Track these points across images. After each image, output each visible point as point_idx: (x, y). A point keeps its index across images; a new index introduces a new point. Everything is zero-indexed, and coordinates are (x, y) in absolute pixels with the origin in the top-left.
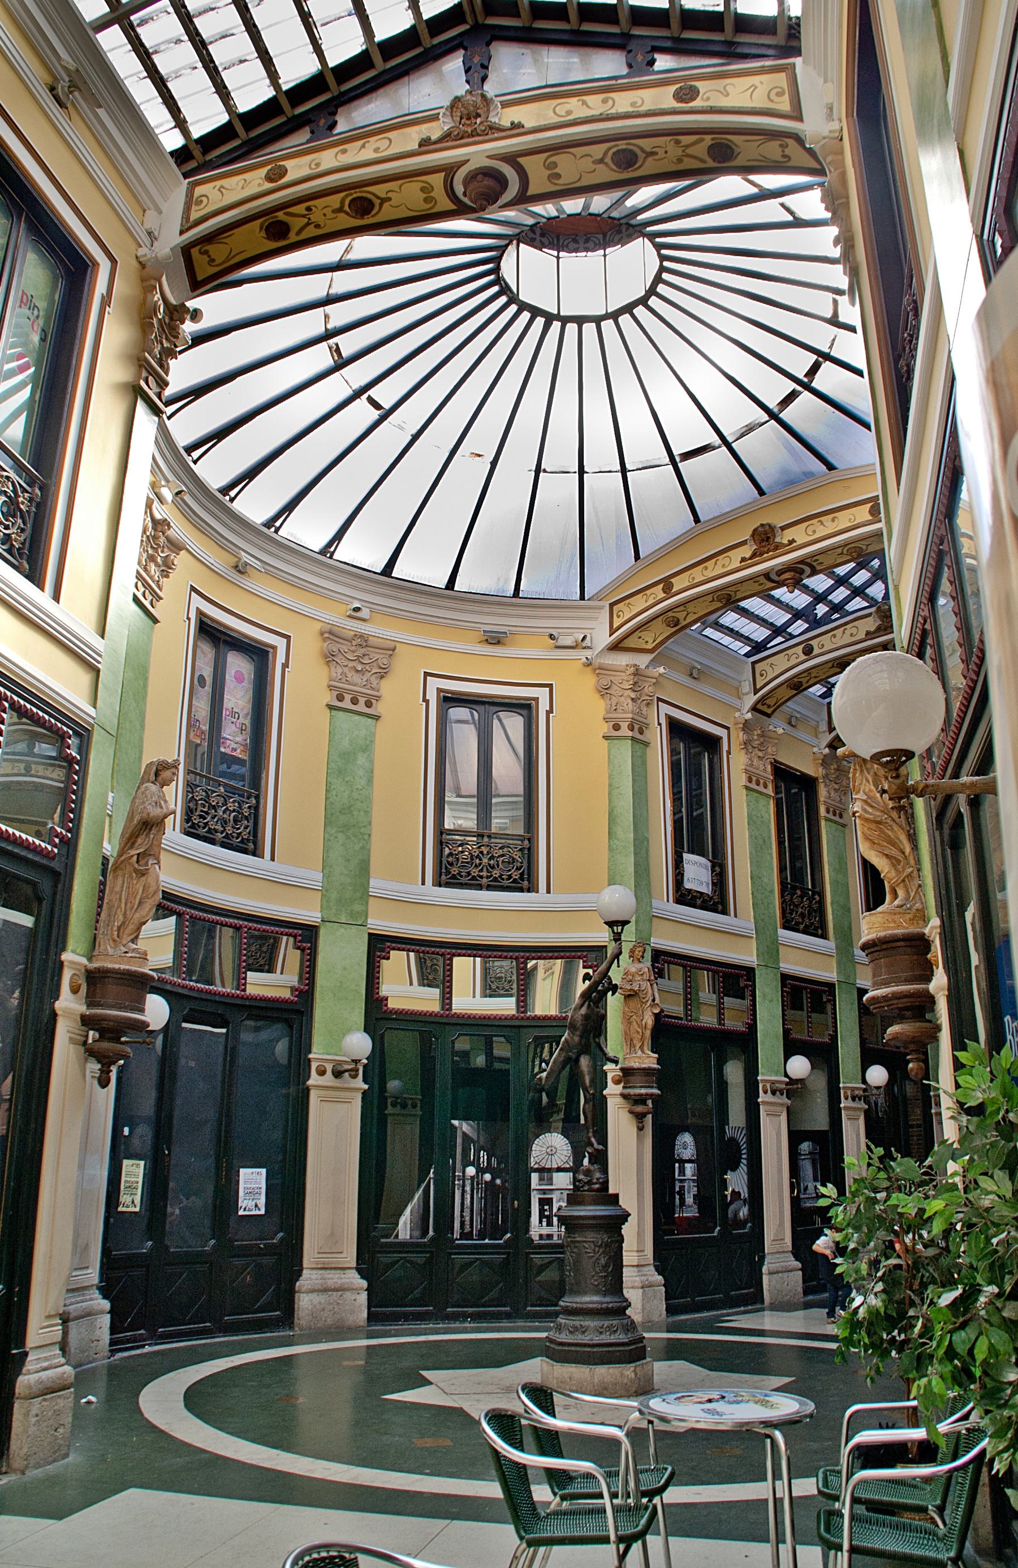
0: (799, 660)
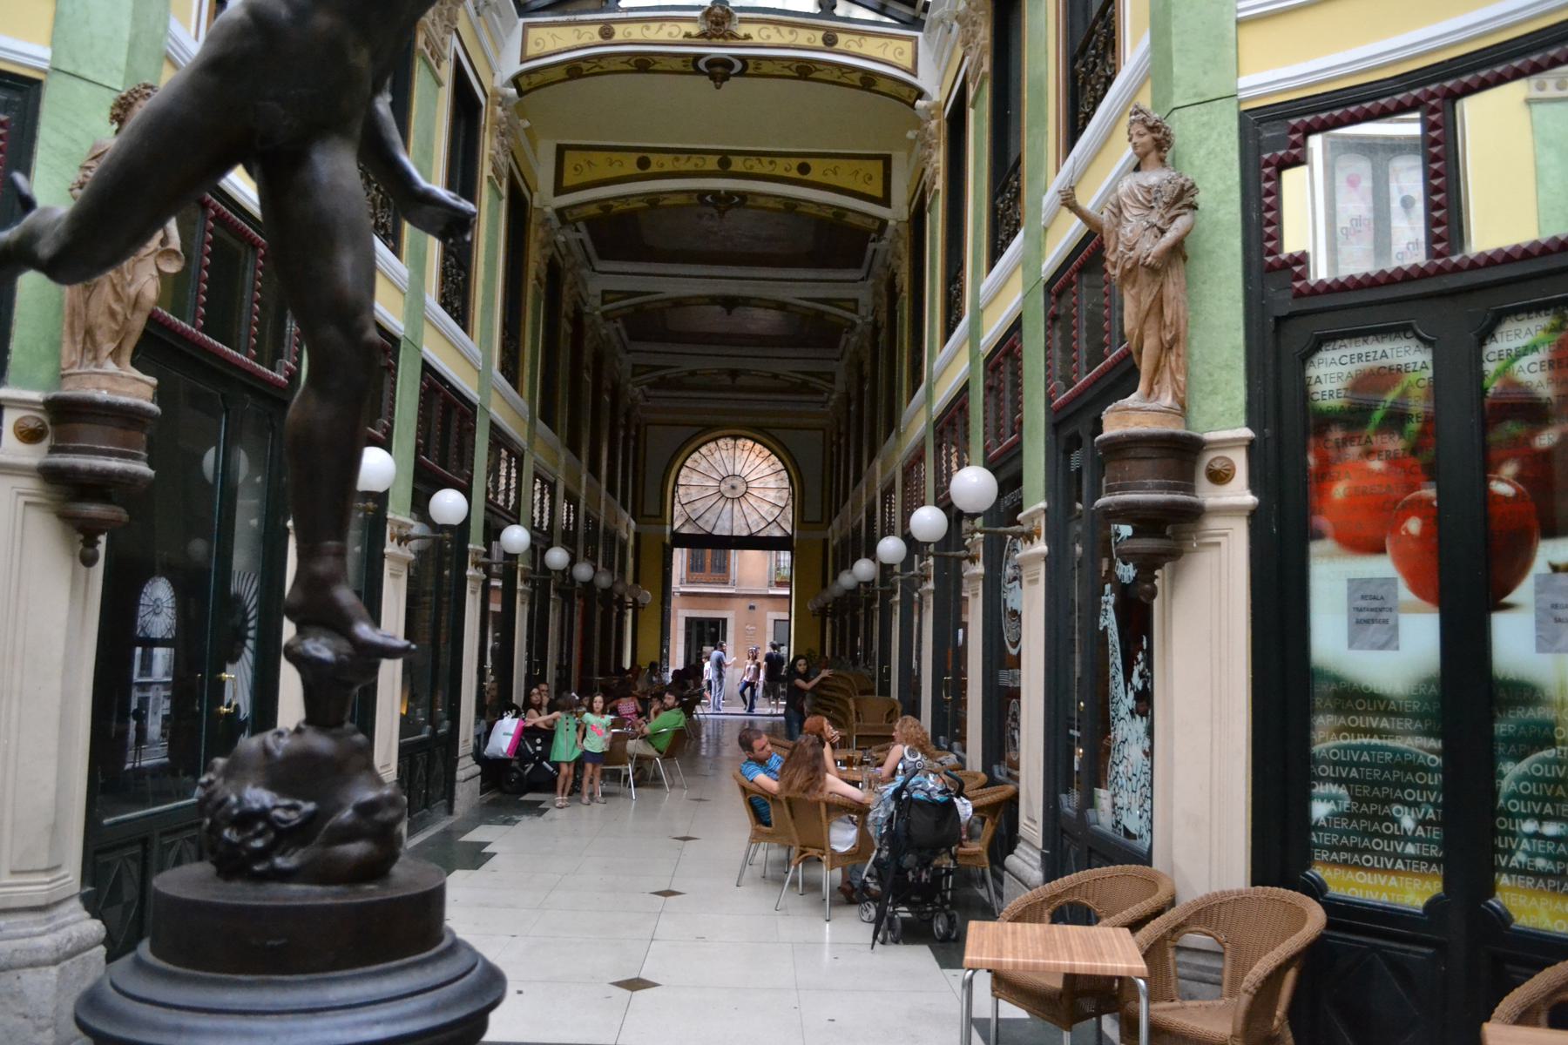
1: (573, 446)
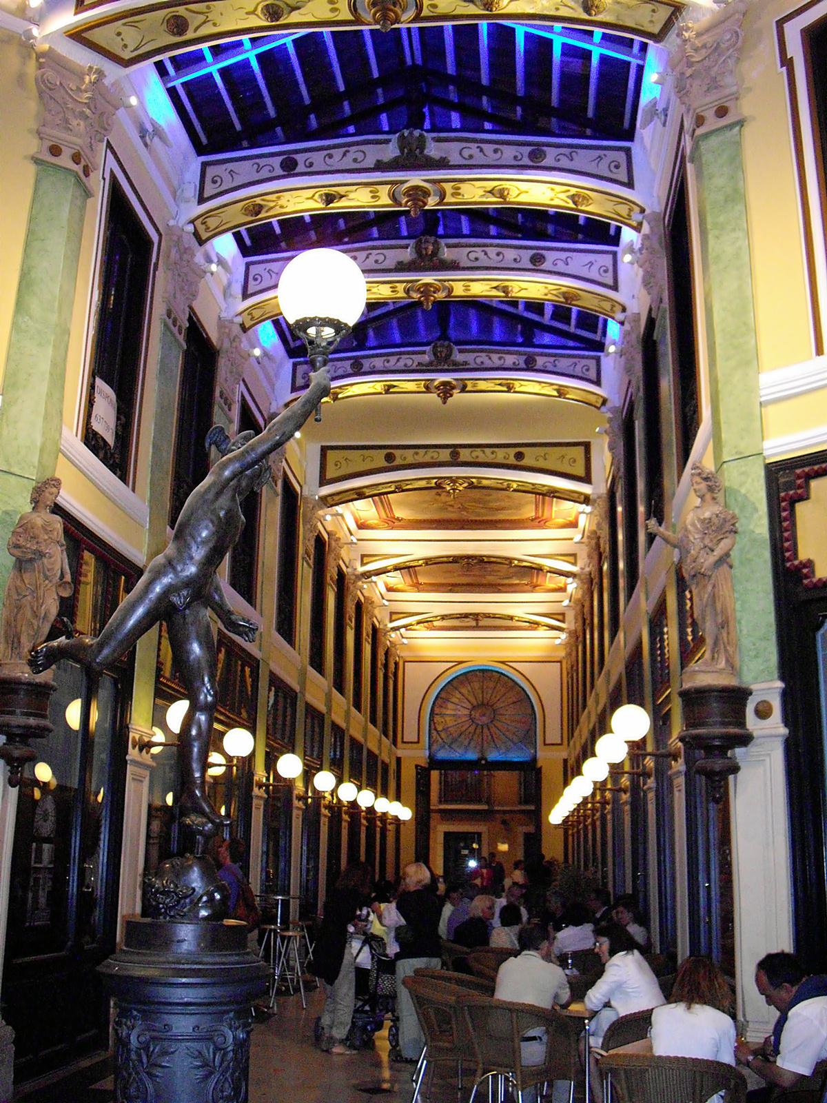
0: (274, 174)
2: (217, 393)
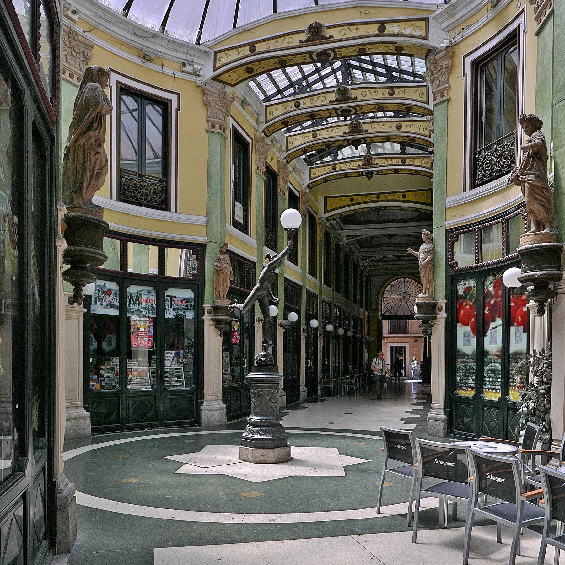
1: (338, 290)
2: (279, 191)
